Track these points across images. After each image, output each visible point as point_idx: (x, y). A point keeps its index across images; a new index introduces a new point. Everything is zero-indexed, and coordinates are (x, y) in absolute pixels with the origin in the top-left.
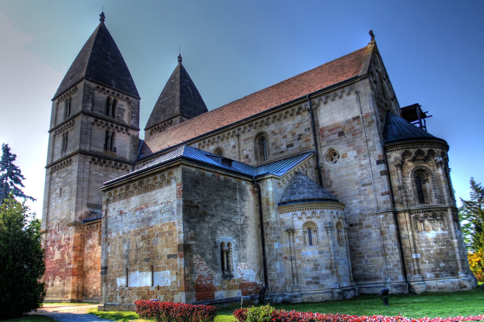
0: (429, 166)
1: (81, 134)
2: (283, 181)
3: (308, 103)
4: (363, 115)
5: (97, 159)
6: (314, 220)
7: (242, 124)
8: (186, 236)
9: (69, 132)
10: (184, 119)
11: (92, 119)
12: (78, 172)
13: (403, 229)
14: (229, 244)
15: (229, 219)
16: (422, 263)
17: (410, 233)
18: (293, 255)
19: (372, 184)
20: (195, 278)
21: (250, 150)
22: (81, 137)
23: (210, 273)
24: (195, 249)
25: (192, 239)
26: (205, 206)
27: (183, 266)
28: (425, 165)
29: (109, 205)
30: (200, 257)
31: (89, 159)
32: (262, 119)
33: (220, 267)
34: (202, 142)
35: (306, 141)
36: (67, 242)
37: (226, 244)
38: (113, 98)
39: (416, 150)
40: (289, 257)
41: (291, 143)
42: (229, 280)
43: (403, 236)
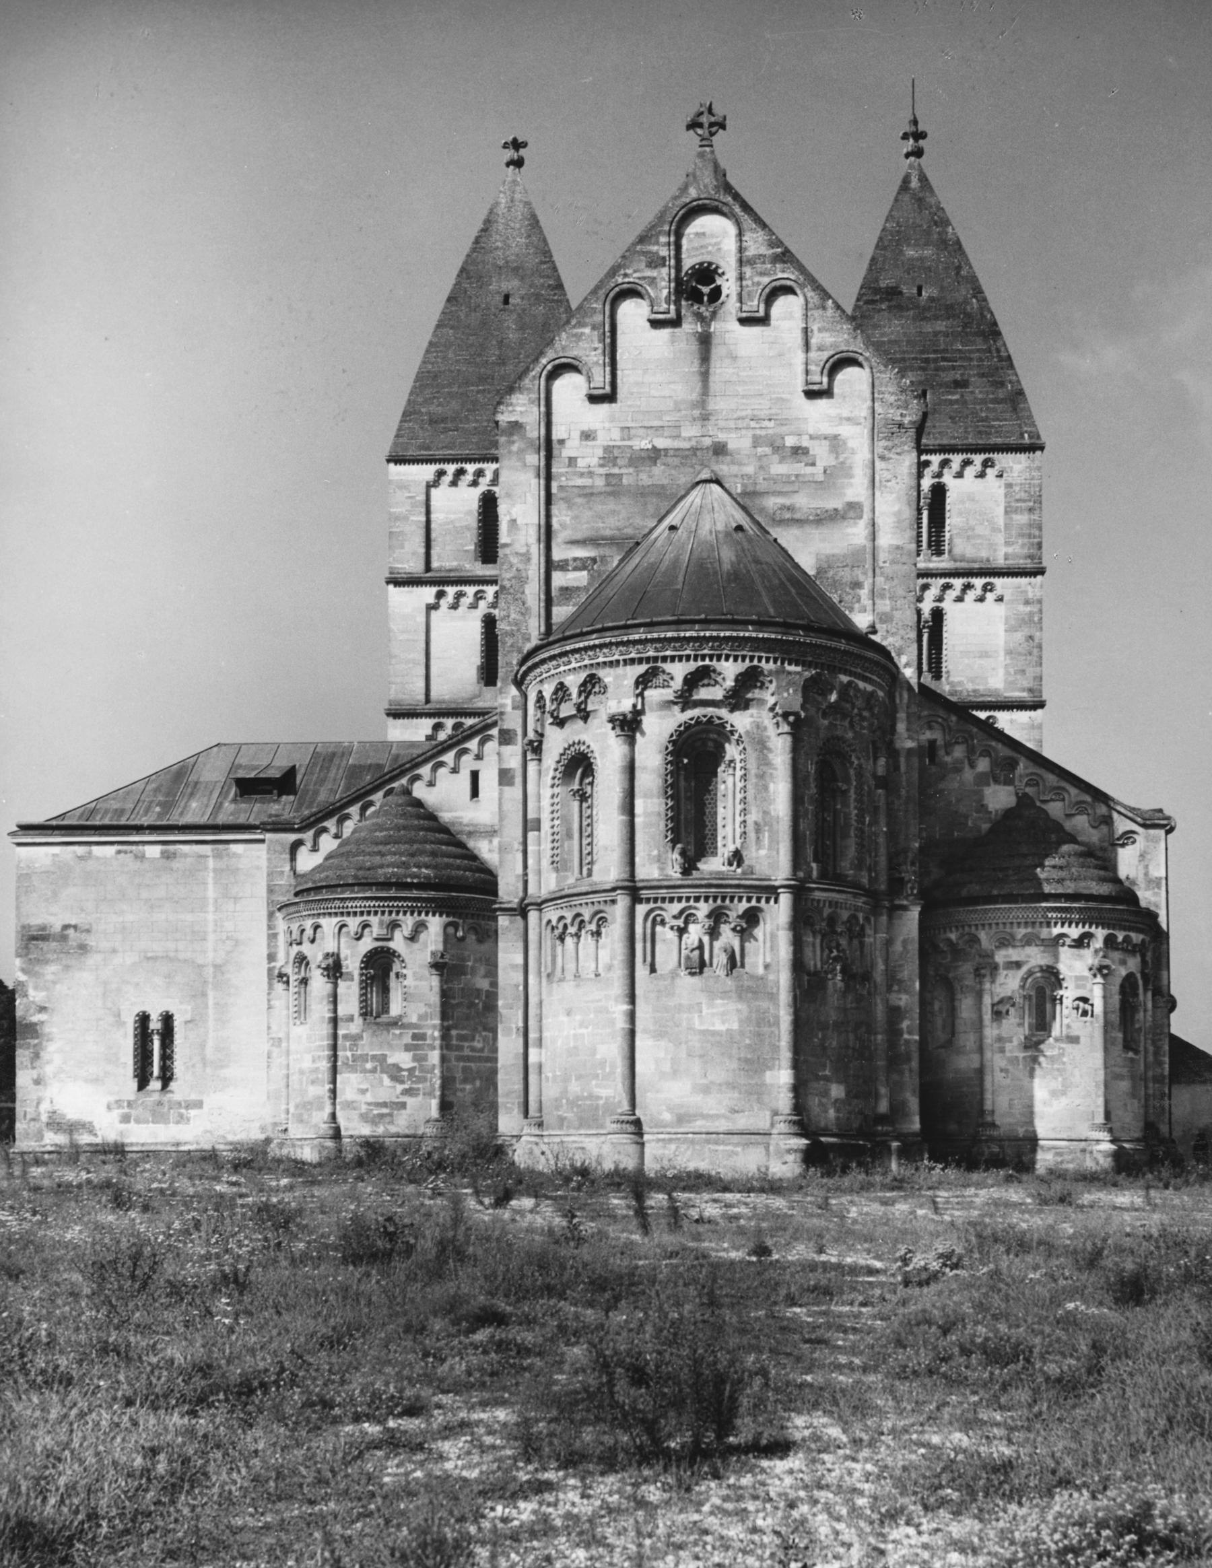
11: (428, 594)
15: (172, 954)
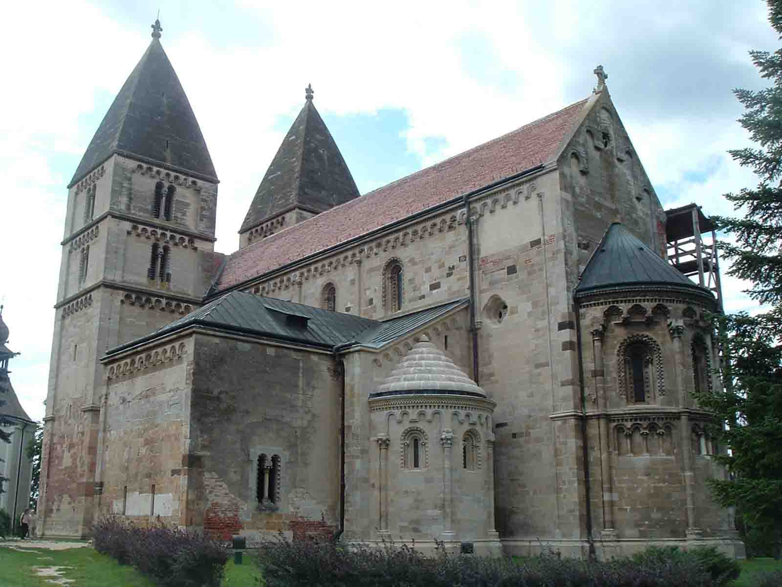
0: (657, 335)
1: (107, 252)
2: (387, 356)
3: (465, 210)
4: (546, 237)
5: (134, 296)
6: (421, 425)
7: (365, 243)
8: (193, 443)
9: (91, 247)
10: (305, 213)
11: (127, 226)
12: (101, 320)
13: (593, 448)
14: (275, 459)
15: (280, 418)
16: (621, 509)
17: (604, 456)
18: (383, 482)
19: (548, 365)
20: (204, 507)
21: (375, 290)
22: (106, 258)
23: (235, 501)
24: (207, 463)
25: (204, 447)
26: (234, 397)
27: (186, 488)
28: (647, 333)
29: (110, 385)
30: (216, 476)
31: (121, 295)
32: (396, 235)
33: (253, 493)
34: (305, 270)
35: (458, 280)
36: (80, 440)
37: (269, 458)
38: (166, 184)
39: (630, 305)
40: (377, 485)
41: (437, 281)
42: (270, 515)
43: (592, 460)
